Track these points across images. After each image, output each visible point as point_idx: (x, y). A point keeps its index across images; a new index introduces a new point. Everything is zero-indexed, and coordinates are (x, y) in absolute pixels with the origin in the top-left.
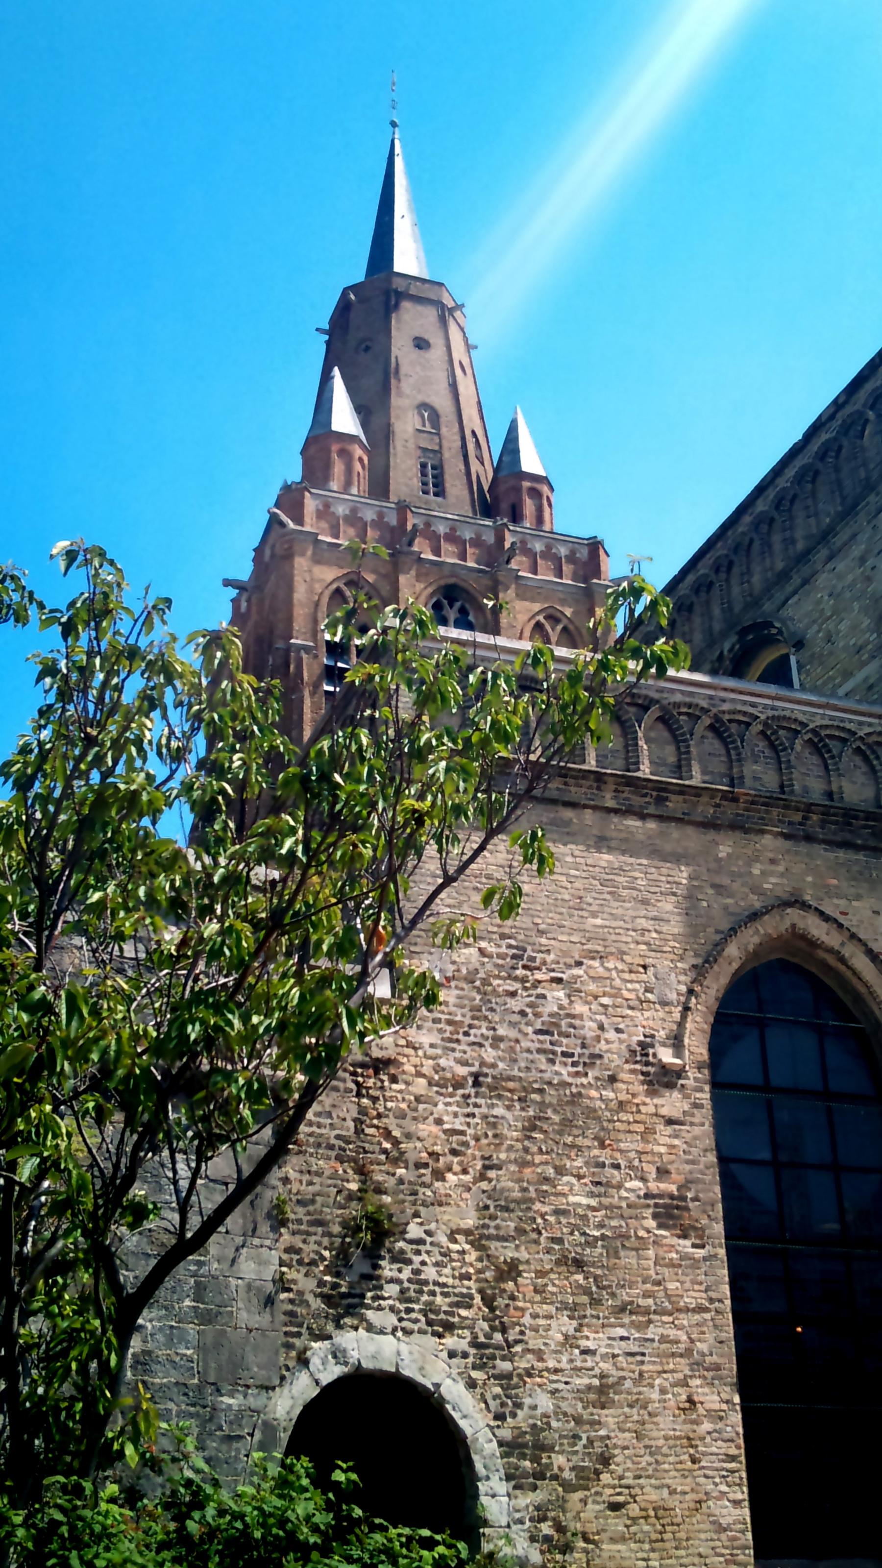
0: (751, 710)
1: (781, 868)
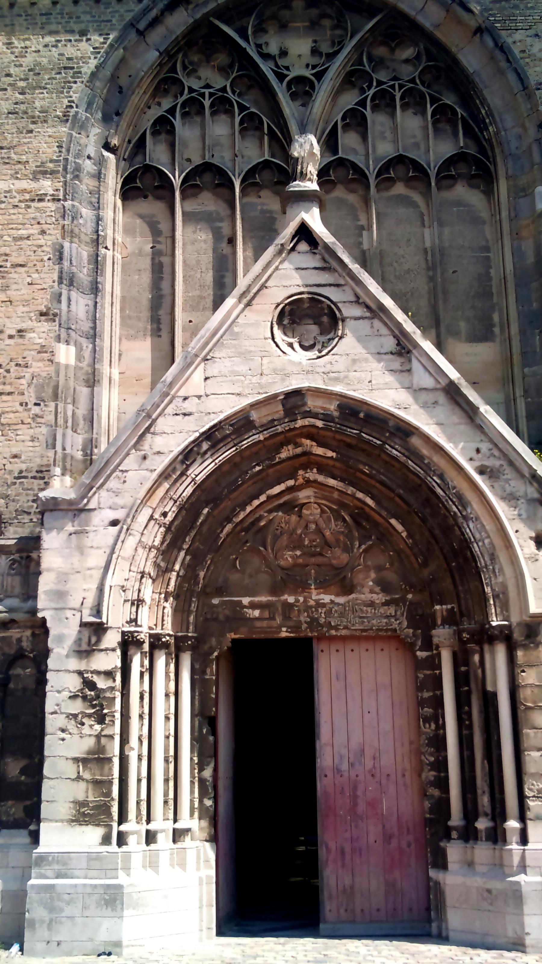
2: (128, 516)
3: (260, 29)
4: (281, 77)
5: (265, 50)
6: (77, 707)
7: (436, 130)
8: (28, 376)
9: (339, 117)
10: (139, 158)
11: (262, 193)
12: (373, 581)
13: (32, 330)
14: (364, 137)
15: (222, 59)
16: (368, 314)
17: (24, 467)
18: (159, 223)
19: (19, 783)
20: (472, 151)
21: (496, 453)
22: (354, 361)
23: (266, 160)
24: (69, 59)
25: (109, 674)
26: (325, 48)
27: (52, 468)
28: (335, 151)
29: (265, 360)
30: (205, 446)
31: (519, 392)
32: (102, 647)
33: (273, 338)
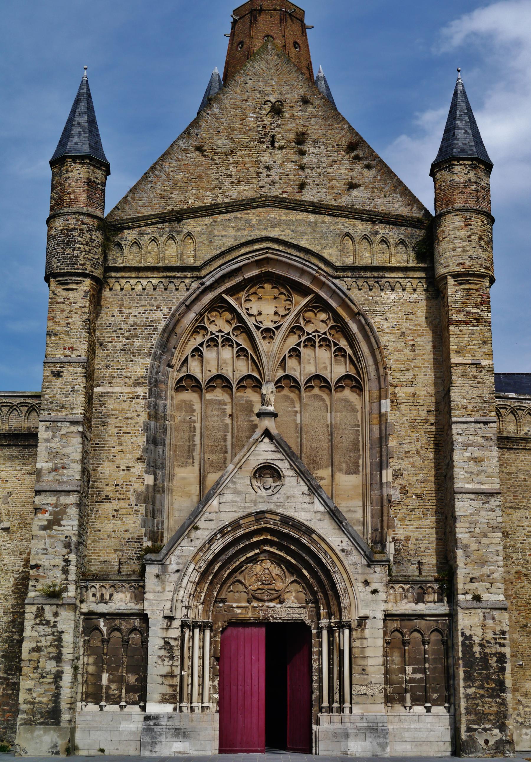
2: (184, 568)
4: (258, 328)
5: (251, 312)
6: (163, 652)
7: (336, 361)
8: (132, 491)
10: (184, 369)
11: (246, 391)
12: (294, 597)
13: (134, 467)
14: (300, 363)
15: (228, 315)
19: (134, 685)
20: (353, 372)
21: (349, 543)
22: (288, 497)
23: (249, 375)
24: (151, 321)
25: (175, 639)
26: (282, 312)
27: (144, 537)
28: (285, 370)
29: (247, 496)
31: (369, 503)
32: (173, 626)
33: (252, 485)
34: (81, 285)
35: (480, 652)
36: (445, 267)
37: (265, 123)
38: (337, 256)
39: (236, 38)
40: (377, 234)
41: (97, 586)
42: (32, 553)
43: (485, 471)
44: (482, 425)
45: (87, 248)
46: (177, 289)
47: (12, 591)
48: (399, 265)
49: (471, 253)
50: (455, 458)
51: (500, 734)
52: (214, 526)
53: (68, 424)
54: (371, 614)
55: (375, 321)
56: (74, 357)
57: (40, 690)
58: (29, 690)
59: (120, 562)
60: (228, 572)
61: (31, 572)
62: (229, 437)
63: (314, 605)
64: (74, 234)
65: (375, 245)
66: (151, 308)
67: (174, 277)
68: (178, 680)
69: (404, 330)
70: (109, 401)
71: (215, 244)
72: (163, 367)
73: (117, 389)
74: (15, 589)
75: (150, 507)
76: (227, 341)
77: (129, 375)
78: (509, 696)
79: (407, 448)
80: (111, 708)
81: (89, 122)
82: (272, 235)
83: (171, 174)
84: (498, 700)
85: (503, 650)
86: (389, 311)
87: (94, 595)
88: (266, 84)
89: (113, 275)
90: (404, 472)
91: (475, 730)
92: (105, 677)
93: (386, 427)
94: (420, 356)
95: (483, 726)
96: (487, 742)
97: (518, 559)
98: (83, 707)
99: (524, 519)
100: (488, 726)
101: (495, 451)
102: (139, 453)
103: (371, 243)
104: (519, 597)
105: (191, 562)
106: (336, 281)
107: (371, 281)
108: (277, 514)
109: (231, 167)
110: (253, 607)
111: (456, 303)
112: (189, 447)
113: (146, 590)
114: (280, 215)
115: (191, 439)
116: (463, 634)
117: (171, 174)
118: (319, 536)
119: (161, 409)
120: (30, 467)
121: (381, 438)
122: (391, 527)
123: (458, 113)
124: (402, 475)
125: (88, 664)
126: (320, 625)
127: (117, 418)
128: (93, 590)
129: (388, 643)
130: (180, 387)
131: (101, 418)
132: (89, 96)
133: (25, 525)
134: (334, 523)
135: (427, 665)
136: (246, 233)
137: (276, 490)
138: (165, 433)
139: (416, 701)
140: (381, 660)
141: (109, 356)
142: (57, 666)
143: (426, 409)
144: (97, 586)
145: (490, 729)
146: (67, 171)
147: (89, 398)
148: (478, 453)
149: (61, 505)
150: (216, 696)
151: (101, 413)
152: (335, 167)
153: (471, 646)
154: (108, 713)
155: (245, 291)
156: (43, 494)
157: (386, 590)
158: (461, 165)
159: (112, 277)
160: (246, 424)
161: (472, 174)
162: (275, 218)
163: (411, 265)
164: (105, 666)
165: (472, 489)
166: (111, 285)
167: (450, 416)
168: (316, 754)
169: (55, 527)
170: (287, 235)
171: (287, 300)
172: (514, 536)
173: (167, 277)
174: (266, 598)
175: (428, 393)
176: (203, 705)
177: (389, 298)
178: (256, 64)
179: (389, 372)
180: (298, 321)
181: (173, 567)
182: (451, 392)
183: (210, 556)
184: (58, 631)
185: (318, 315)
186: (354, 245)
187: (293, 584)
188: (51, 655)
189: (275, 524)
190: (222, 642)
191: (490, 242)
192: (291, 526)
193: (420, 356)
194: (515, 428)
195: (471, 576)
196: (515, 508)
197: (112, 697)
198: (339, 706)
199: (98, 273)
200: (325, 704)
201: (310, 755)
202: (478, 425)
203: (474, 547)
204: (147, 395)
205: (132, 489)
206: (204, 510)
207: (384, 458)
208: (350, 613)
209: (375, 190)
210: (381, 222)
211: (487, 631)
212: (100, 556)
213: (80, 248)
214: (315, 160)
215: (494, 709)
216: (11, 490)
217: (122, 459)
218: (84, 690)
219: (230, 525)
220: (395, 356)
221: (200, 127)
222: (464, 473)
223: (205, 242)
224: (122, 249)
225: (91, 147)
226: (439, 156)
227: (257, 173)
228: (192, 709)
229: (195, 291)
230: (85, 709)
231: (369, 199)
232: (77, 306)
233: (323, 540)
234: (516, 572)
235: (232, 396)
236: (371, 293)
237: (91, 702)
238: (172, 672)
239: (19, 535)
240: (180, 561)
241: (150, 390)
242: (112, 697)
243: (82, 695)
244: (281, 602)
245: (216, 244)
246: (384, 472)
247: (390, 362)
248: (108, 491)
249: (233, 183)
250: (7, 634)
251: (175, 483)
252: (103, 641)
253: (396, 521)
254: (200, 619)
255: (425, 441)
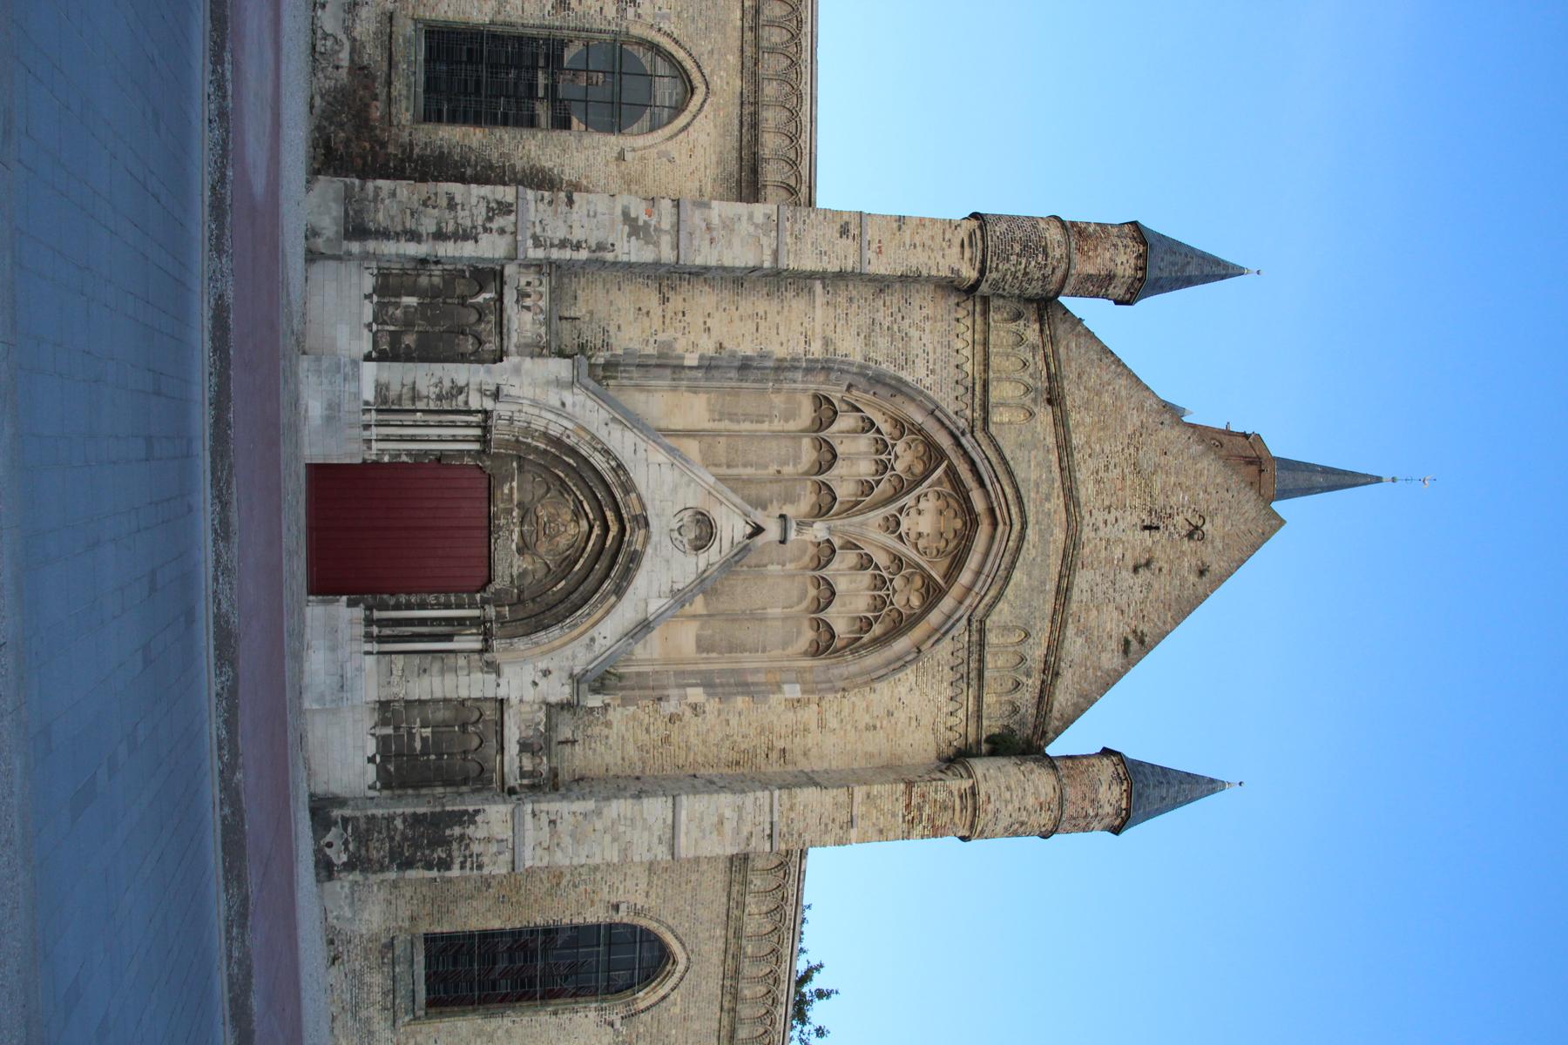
0: (803, 81)
1: (725, 87)
3: (939, 495)
4: (901, 510)
6: (447, 384)
7: (854, 619)
8: (676, 335)
9: (866, 551)
10: (845, 407)
15: (918, 468)
16: (699, 571)
17: (611, 333)
18: (794, 420)
20: (838, 643)
21: (603, 649)
22: (668, 561)
25: (466, 403)
26: (922, 543)
27: (610, 353)
28: (842, 548)
29: (670, 504)
30: (613, 463)
31: (657, 668)
32: (484, 399)
33: (686, 509)
34: (968, 264)
35: (452, 835)
36: (985, 775)
37: (1176, 517)
38: (999, 622)
39: (1227, 437)
40: (1027, 676)
41: (540, 289)
42: (591, 197)
43: (704, 838)
44: (768, 832)
45: (1019, 275)
46: (957, 398)
47: (534, 165)
48: (985, 706)
49: (1003, 811)
50: (722, 796)
51: (341, 862)
52: (626, 456)
53: (774, 246)
54: (503, 681)
55: (909, 675)
56: (869, 254)
57: (394, 211)
58: (393, 194)
59: (575, 319)
60: (562, 475)
61: (562, 195)
62: (749, 471)
63: (515, 596)
64: (1040, 256)
65: (1013, 674)
66: (931, 361)
67: (973, 394)
68: (407, 408)
69: (895, 715)
70: (803, 301)
71: (1018, 451)
72: (848, 379)
73: (819, 312)
74: (537, 169)
75: (653, 362)
76: (884, 467)
77: (838, 330)
78: (392, 875)
79: (734, 721)
80: (368, 311)
81: (1190, 277)
82: (1029, 532)
83: (1111, 388)
84: (387, 860)
85: (456, 866)
86: (923, 693)
87: (529, 284)
88: (1227, 518)
89: (978, 308)
90: (700, 719)
91: (345, 829)
92: (412, 301)
93: (763, 692)
94: (860, 737)
95: (350, 839)
96: (330, 845)
97: (580, 874)
98: (370, 271)
99: (634, 882)
100: (351, 847)
101: (731, 850)
102: (729, 345)
103: (1015, 668)
104: (527, 876)
105: (576, 424)
106: (964, 621)
107: (963, 669)
108: (645, 544)
109: (1119, 470)
110: (512, 510)
111: (936, 792)
112: (736, 414)
113: (536, 360)
114: (1055, 541)
115: (747, 417)
116: (477, 812)
117: (1111, 388)
118: (613, 606)
119: (790, 375)
120: (709, 189)
121: (747, 685)
122: (625, 703)
123: (1187, 787)
124: (696, 715)
125: (430, 276)
126: (486, 607)
127: (778, 313)
128: (537, 283)
129: (463, 702)
130: (821, 401)
131: (778, 290)
132: (1223, 277)
133: (628, 182)
134: (631, 627)
135: (433, 757)
136: (1033, 495)
137: (677, 543)
138: (755, 381)
139: (383, 742)
140: (438, 694)
141: (866, 301)
142: (428, 234)
143: (787, 748)
144: (540, 289)
145: (346, 849)
146: (1126, 247)
147: (812, 276)
148: (728, 827)
149: (659, 237)
150: (386, 459)
151: (786, 290)
152: (1115, 614)
153: (461, 823)
154: (361, 306)
155: (951, 492)
156: (674, 210)
157: (537, 701)
158: (1121, 794)
159: (974, 305)
160: (766, 493)
161: (1108, 809)
162: (1052, 535)
163: (985, 723)
164: (427, 301)
165: (680, 820)
166: (963, 305)
167: (780, 788)
168: (309, 601)
169: (626, 228)
170: (1029, 552)
171: (938, 551)
172: (611, 869)
173: (974, 384)
174: (526, 527)
175: (809, 750)
176: (373, 442)
177: (940, 693)
178: (1252, 503)
179: (839, 696)
180: (909, 565)
181: (568, 397)
182: (814, 788)
183: (585, 450)
184: (477, 234)
185: (916, 593)
186: (1013, 645)
187: (543, 565)
188: (444, 225)
189: (630, 543)
190: (462, 467)
191: (1015, 834)
192: (628, 567)
193: (860, 737)
194: (760, 867)
195: (559, 821)
196: (649, 870)
197: (384, 312)
198: (375, 634)
199: (984, 288)
200: (377, 614)
201: (305, 590)
202: (767, 826)
203: (599, 825)
204: (810, 357)
205: (679, 335)
206: (650, 442)
207: (720, 690)
208: (505, 650)
209: (1083, 669)
210: (1043, 682)
211: (482, 845)
212: (583, 290)
213: (1020, 264)
214: (1125, 585)
215: (374, 855)
216: (678, 162)
217: (721, 321)
218: (394, 271)
219: (629, 478)
220: (861, 704)
221: (1172, 427)
222: (702, 809)
223: (1021, 437)
224: (1014, 320)
225: (1158, 279)
226: (1133, 762)
227: (1109, 507)
228: (367, 427)
229: (954, 423)
230: (366, 274)
231: (1072, 661)
232: (939, 259)
233: (608, 612)
234: (562, 873)
235: (807, 473)
236: (947, 669)
237: (377, 282)
238: (420, 398)
239: (614, 173)
240: (577, 408)
241: (817, 361)
242: (384, 312)
243: (387, 269)
244: (520, 551)
245: (1018, 454)
246: (700, 690)
247: (853, 697)
248: (676, 302)
249: (1097, 473)
250: (473, 158)
251: (686, 394)
252: (463, 298)
253: (632, 709)
254: (495, 435)
255: (743, 747)
